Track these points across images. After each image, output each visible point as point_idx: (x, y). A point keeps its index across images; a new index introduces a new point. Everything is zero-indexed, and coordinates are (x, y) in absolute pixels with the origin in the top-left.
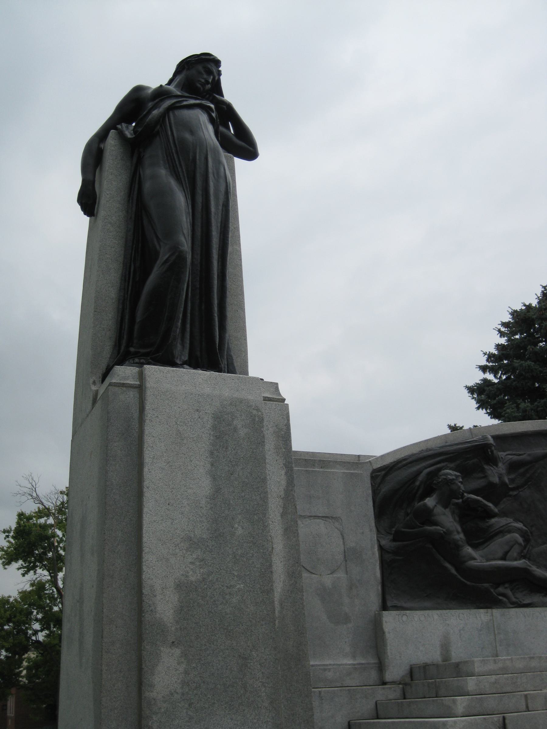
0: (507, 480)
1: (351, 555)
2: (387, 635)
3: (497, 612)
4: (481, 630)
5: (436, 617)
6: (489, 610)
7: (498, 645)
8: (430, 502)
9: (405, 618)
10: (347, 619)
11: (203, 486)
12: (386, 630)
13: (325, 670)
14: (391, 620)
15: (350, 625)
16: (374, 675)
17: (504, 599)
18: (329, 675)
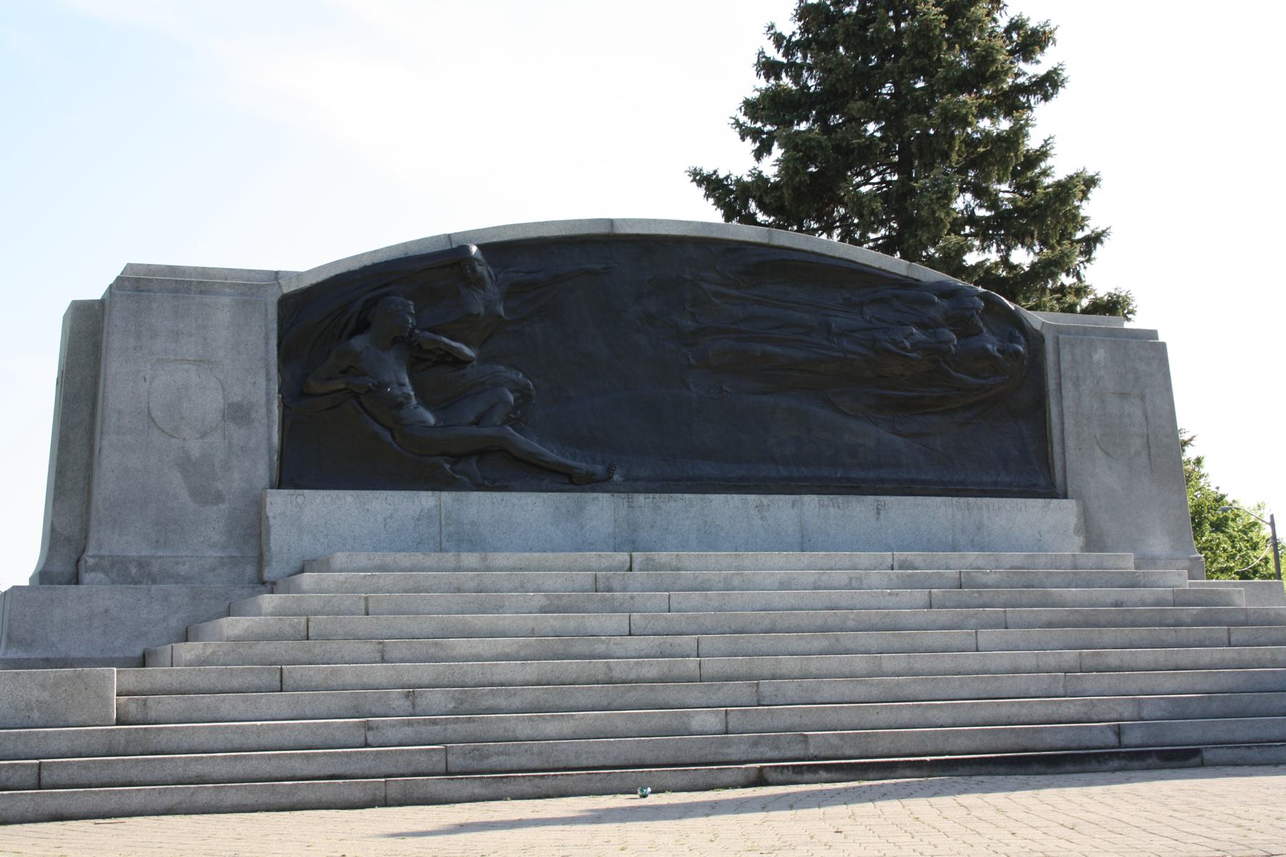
0: (501, 310)
1: (237, 413)
2: (272, 521)
3: (446, 496)
4: (419, 519)
5: (349, 499)
6: (437, 493)
7: (444, 540)
8: (359, 343)
9: (300, 500)
10: (219, 498)
12: (270, 514)
13: (177, 563)
14: (280, 503)
15: (223, 507)
16: (250, 571)
17: (465, 479)
18: (183, 569)
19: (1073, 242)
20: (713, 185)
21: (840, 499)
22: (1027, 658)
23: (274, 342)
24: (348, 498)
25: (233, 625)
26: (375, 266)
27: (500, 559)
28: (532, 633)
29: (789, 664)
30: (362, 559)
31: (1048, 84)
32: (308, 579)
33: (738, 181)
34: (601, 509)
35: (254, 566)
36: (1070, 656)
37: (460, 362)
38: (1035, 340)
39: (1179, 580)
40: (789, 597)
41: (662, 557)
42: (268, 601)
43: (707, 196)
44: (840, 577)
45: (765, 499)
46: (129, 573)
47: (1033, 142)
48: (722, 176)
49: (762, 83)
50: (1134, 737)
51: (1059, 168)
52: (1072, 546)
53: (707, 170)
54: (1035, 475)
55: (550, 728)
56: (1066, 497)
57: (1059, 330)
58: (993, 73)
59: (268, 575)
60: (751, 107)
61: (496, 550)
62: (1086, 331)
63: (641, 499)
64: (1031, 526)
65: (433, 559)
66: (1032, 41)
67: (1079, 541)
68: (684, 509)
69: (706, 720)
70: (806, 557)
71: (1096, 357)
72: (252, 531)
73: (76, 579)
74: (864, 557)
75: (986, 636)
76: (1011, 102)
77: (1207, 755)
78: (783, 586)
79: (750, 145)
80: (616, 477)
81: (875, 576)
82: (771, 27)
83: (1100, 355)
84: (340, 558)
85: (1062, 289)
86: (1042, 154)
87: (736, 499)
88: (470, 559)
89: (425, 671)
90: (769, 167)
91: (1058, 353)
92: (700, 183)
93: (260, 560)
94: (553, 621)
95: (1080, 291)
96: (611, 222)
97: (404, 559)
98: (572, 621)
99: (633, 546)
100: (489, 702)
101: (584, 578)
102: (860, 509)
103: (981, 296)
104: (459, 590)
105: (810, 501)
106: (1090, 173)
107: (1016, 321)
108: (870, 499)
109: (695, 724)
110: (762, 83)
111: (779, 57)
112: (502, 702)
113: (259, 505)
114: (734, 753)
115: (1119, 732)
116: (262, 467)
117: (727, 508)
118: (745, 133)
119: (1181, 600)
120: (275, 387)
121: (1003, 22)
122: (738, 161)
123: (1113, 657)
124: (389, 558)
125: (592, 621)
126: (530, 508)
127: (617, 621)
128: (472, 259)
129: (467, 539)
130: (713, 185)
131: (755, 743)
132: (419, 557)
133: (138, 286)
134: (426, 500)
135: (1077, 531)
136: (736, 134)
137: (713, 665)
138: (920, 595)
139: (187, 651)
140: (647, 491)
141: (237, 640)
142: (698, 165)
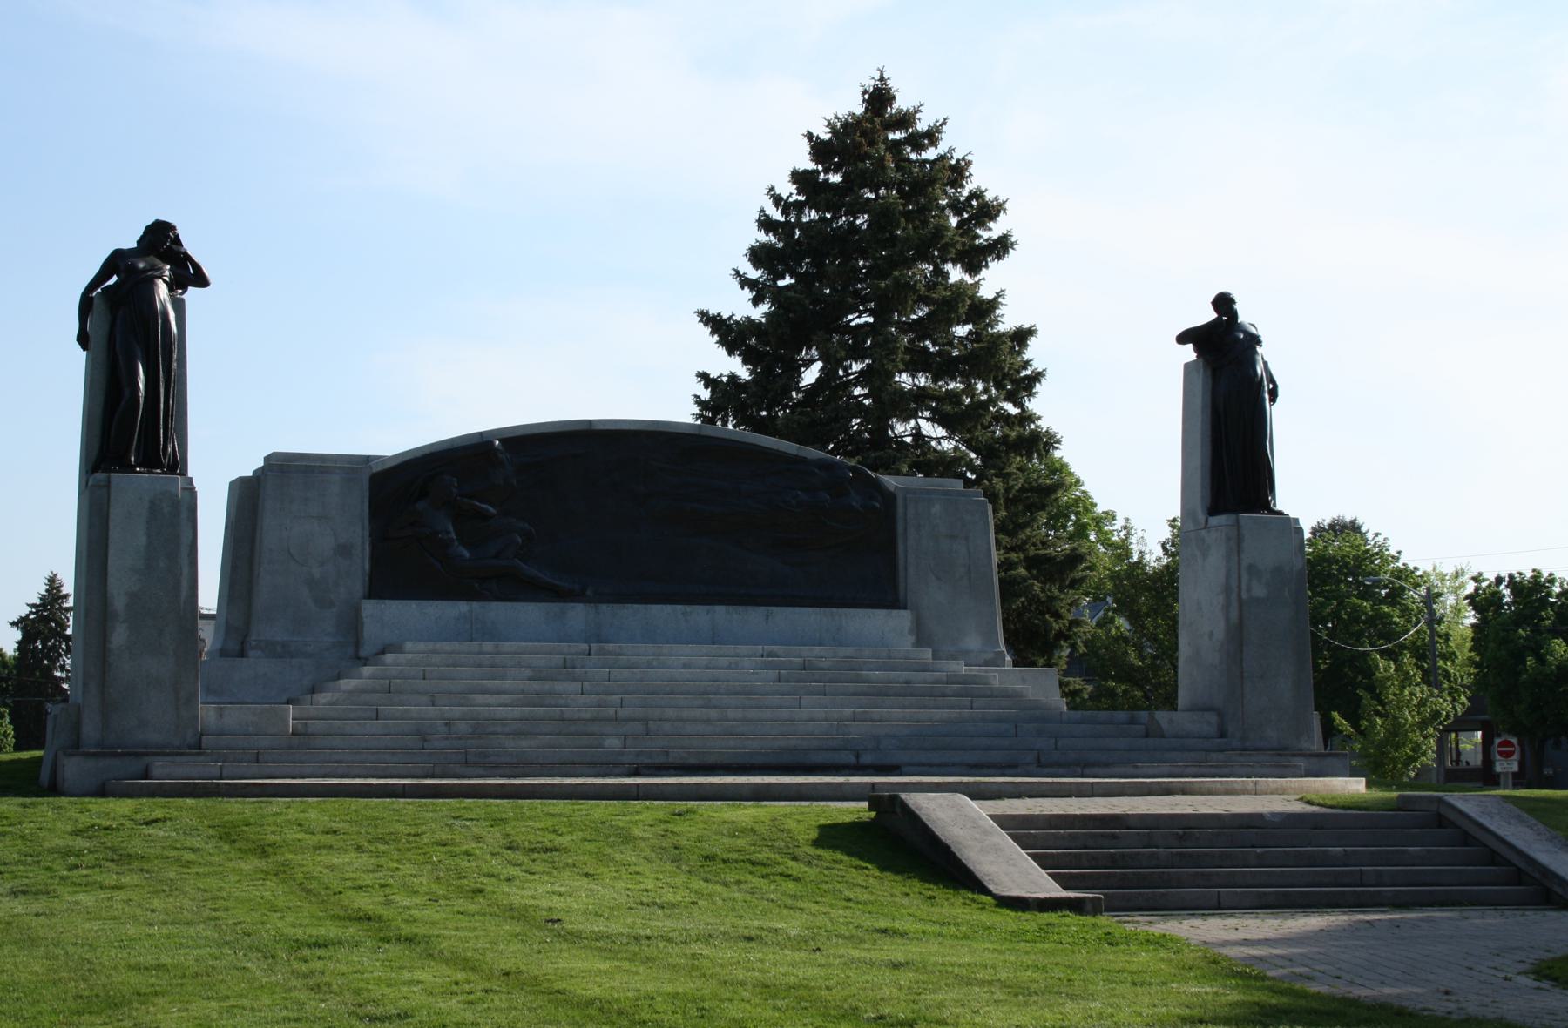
1: (344, 550)
3: (475, 605)
8: (421, 505)
11: (143, 540)
14: (370, 608)
19: (1015, 382)
20: (717, 324)
21: (741, 608)
22: (819, 712)
23: (367, 504)
24: (413, 605)
25: (347, 684)
26: (432, 454)
27: (507, 646)
28: (523, 692)
29: (670, 712)
30: (422, 646)
31: (1001, 247)
32: (389, 657)
33: (737, 322)
34: (578, 614)
35: (354, 649)
36: (848, 712)
37: (485, 517)
38: (889, 498)
39: (961, 668)
40: (686, 673)
41: (610, 647)
42: (367, 670)
43: (712, 334)
44: (723, 661)
45: (688, 608)
46: (280, 652)
47: (986, 292)
48: (725, 316)
49: (763, 237)
50: (867, 759)
51: (1008, 320)
52: (906, 644)
53: (713, 312)
54: (883, 591)
55: (524, 743)
56: (905, 608)
57: (907, 491)
58: (947, 244)
59: (362, 653)
60: (758, 255)
61: (507, 640)
62: (928, 492)
63: (604, 607)
64: (881, 628)
65: (465, 646)
66: (988, 211)
67: (912, 639)
68: (633, 615)
69: (613, 742)
70: (705, 648)
71: (933, 510)
72: (352, 626)
73: (242, 654)
74: (743, 649)
75: (805, 700)
76: (974, 259)
77: (904, 769)
78: (685, 666)
79: (748, 294)
80: (589, 592)
81: (746, 662)
82: (772, 189)
83: (937, 509)
84: (409, 645)
85: (1006, 419)
86: (993, 304)
87: (668, 608)
88: (488, 646)
89: (457, 711)
90: (759, 313)
91: (905, 507)
92: (706, 324)
93: (357, 644)
94: (536, 685)
95: (1027, 418)
96: (590, 422)
97: (447, 646)
98: (547, 685)
99: (599, 640)
100: (492, 729)
101: (558, 659)
102: (753, 617)
103: (853, 469)
104: (480, 666)
105: (720, 610)
106: (1027, 326)
107: (877, 485)
108: (762, 609)
109: (607, 743)
110: (763, 237)
111: (777, 215)
112: (499, 729)
113: (357, 610)
114: (625, 759)
115: (857, 757)
116: (358, 584)
117: (661, 613)
118: (745, 282)
119: (952, 679)
120: (367, 533)
121: (966, 193)
122: (740, 306)
123: (876, 713)
124: (439, 645)
125: (559, 686)
126: (530, 613)
127: (575, 686)
128: (495, 450)
129: (490, 633)
130: (717, 324)
131: (638, 754)
132: (456, 645)
133: (281, 468)
134: (463, 607)
135: (910, 632)
136: (736, 283)
137: (624, 712)
138: (773, 674)
139: (323, 698)
140: (609, 602)
141: (350, 692)
142: (705, 309)
